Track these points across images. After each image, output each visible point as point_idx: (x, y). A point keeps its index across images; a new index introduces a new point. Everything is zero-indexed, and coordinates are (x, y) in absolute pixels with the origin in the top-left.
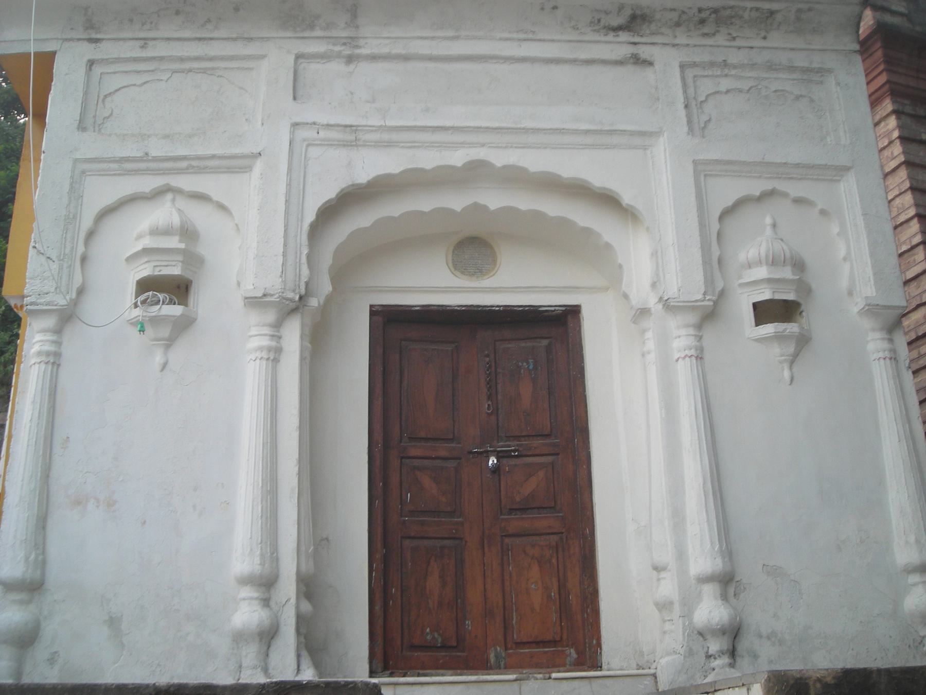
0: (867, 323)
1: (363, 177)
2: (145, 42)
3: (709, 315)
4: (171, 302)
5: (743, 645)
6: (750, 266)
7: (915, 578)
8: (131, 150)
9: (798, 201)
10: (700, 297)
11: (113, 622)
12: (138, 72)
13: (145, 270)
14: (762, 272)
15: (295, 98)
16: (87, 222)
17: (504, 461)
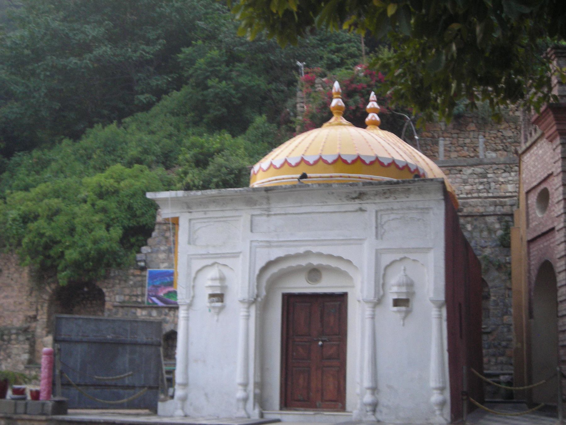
0: (432, 305)
1: (273, 258)
2: (205, 213)
3: (378, 302)
4: (217, 302)
5: (378, 409)
6: (393, 286)
7: (435, 391)
8: (203, 251)
9: (414, 260)
10: (372, 299)
11: (206, 395)
12: (204, 222)
13: (210, 292)
14: (395, 289)
15: (252, 231)
16: (193, 275)
17: (325, 343)
